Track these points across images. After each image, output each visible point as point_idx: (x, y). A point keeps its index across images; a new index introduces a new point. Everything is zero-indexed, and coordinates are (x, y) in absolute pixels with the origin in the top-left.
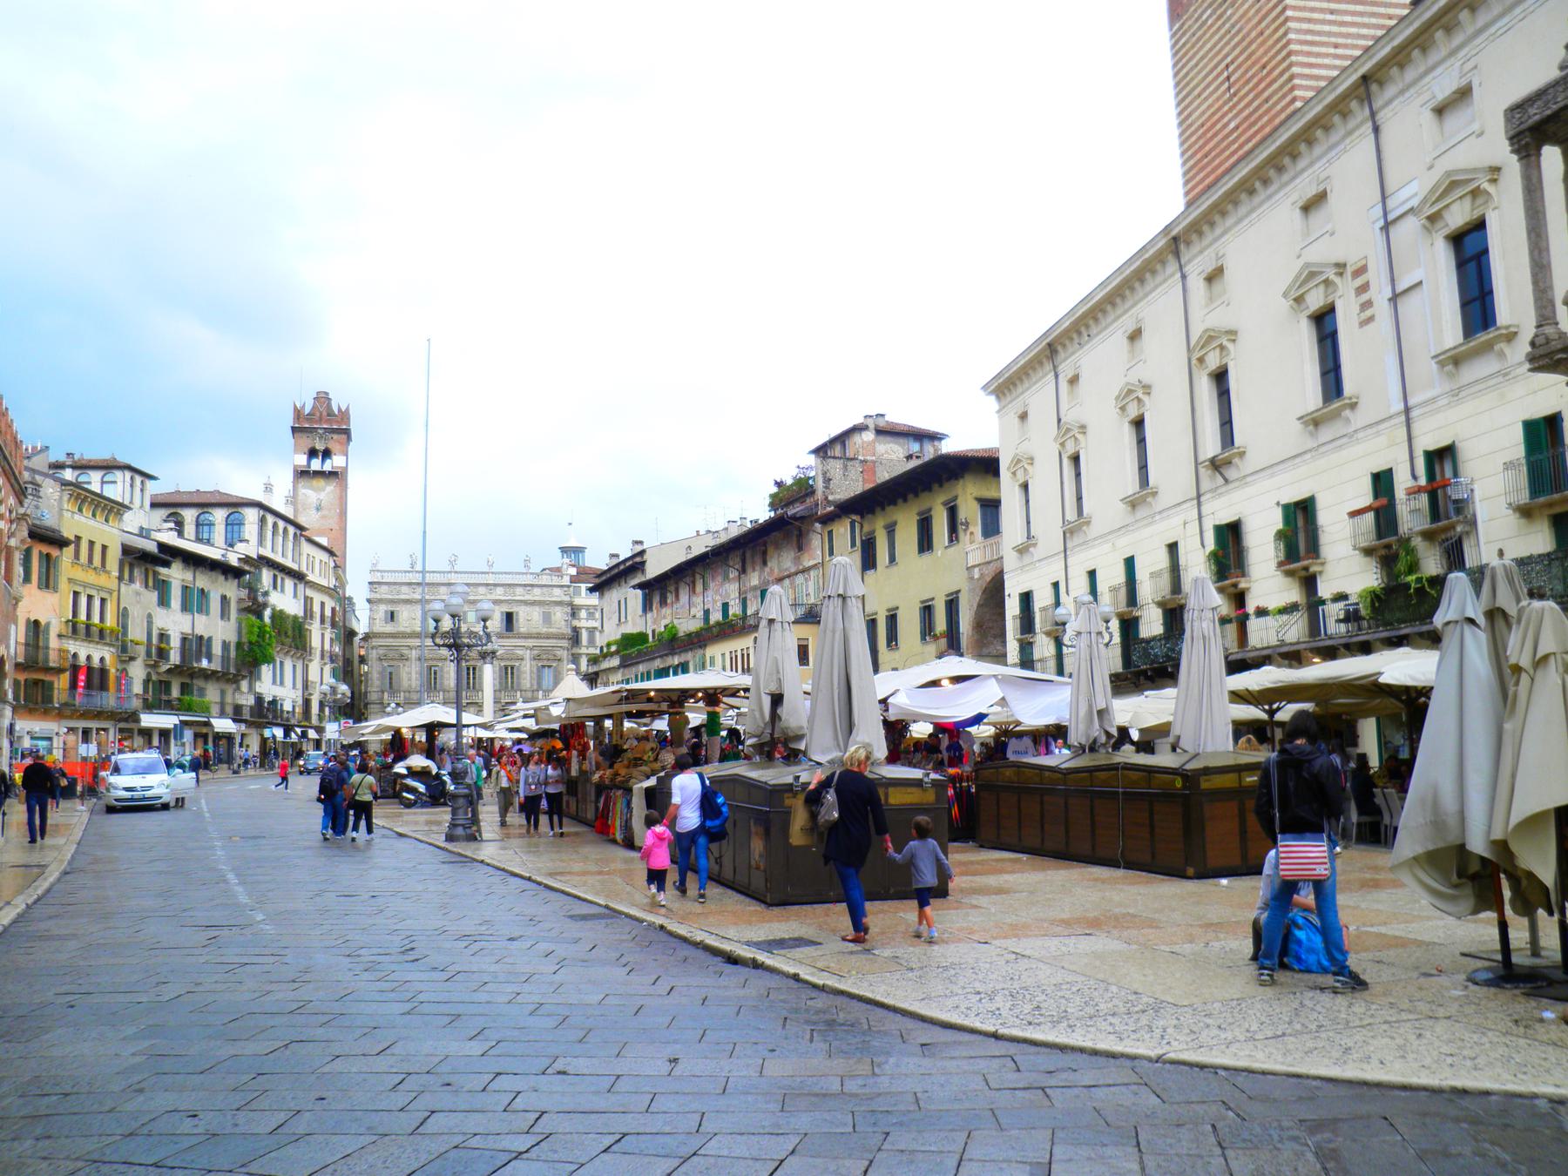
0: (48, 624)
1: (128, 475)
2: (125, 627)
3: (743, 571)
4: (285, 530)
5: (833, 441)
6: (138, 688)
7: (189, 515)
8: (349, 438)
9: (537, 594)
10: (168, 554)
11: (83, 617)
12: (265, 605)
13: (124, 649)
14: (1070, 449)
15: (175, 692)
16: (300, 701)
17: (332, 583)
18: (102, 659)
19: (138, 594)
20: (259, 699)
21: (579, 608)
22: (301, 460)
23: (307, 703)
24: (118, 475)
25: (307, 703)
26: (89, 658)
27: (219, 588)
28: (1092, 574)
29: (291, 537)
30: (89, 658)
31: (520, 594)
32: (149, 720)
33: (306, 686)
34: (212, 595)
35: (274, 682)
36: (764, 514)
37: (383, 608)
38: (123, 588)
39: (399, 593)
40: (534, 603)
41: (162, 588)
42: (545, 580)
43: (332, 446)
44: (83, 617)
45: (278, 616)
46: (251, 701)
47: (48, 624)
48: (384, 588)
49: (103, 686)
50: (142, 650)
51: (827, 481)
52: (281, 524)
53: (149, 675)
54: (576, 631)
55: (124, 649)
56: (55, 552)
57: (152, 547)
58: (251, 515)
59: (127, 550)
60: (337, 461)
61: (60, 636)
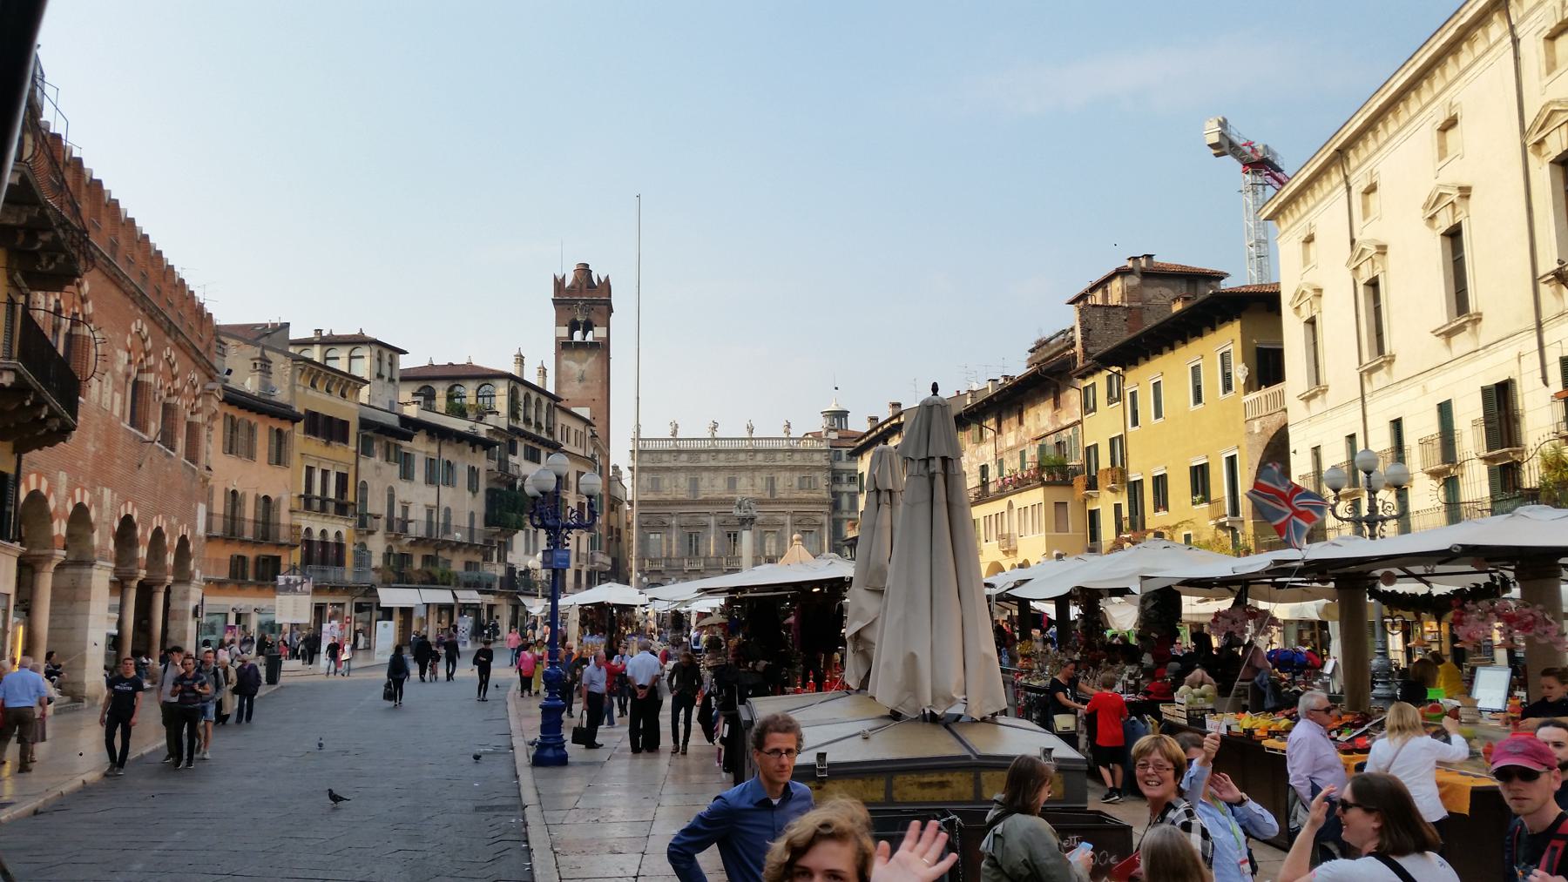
0: (279, 500)
1: (375, 349)
2: (364, 501)
3: (999, 431)
4: (538, 401)
5: (1093, 289)
6: (377, 561)
7: (441, 390)
8: (610, 310)
9: (798, 460)
10: (410, 427)
11: (317, 491)
12: (515, 478)
13: (363, 524)
14: (1365, 274)
15: (417, 564)
17: (590, 452)
18: (338, 534)
19: (378, 467)
20: (511, 570)
21: (843, 471)
22: (564, 332)
24: (364, 351)
26: (324, 532)
27: (464, 460)
28: (1397, 424)
29: (544, 407)
30: (324, 532)
31: (780, 459)
32: (391, 597)
35: (527, 552)
36: (1019, 369)
37: (644, 476)
38: (362, 463)
39: (660, 461)
40: (793, 469)
42: (809, 445)
43: (594, 318)
44: (317, 491)
46: (500, 571)
47: (279, 500)
48: (646, 457)
49: (340, 562)
50: (382, 523)
51: (1086, 332)
52: (534, 395)
53: (390, 548)
54: (836, 495)
55: (363, 524)
56: (286, 427)
57: (393, 421)
58: (502, 389)
59: (365, 424)
60: (598, 333)
61: (291, 511)
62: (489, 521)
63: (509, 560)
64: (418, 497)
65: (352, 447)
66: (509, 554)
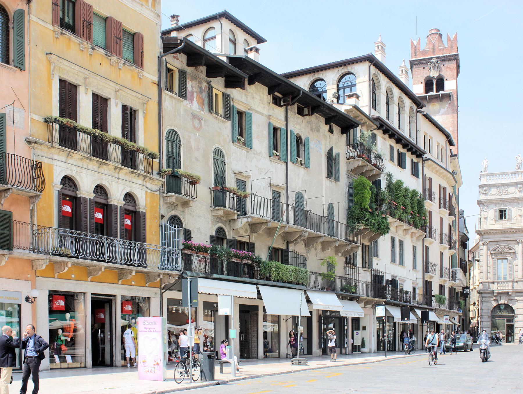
16: (420, 285)
19: (194, 116)
20: (377, 278)
23: (428, 285)
25: (428, 285)
26: (100, 189)
27: (322, 139)
29: (407, 109)
33: (426, 268)
34: (312, 145)
35: (393, 260)
41: (241, 122)
45: (395, 188)
62: (354, 216)
63: (374, 267)
64: (258, 170)
65: (150, 72)
66: (375, 260)
